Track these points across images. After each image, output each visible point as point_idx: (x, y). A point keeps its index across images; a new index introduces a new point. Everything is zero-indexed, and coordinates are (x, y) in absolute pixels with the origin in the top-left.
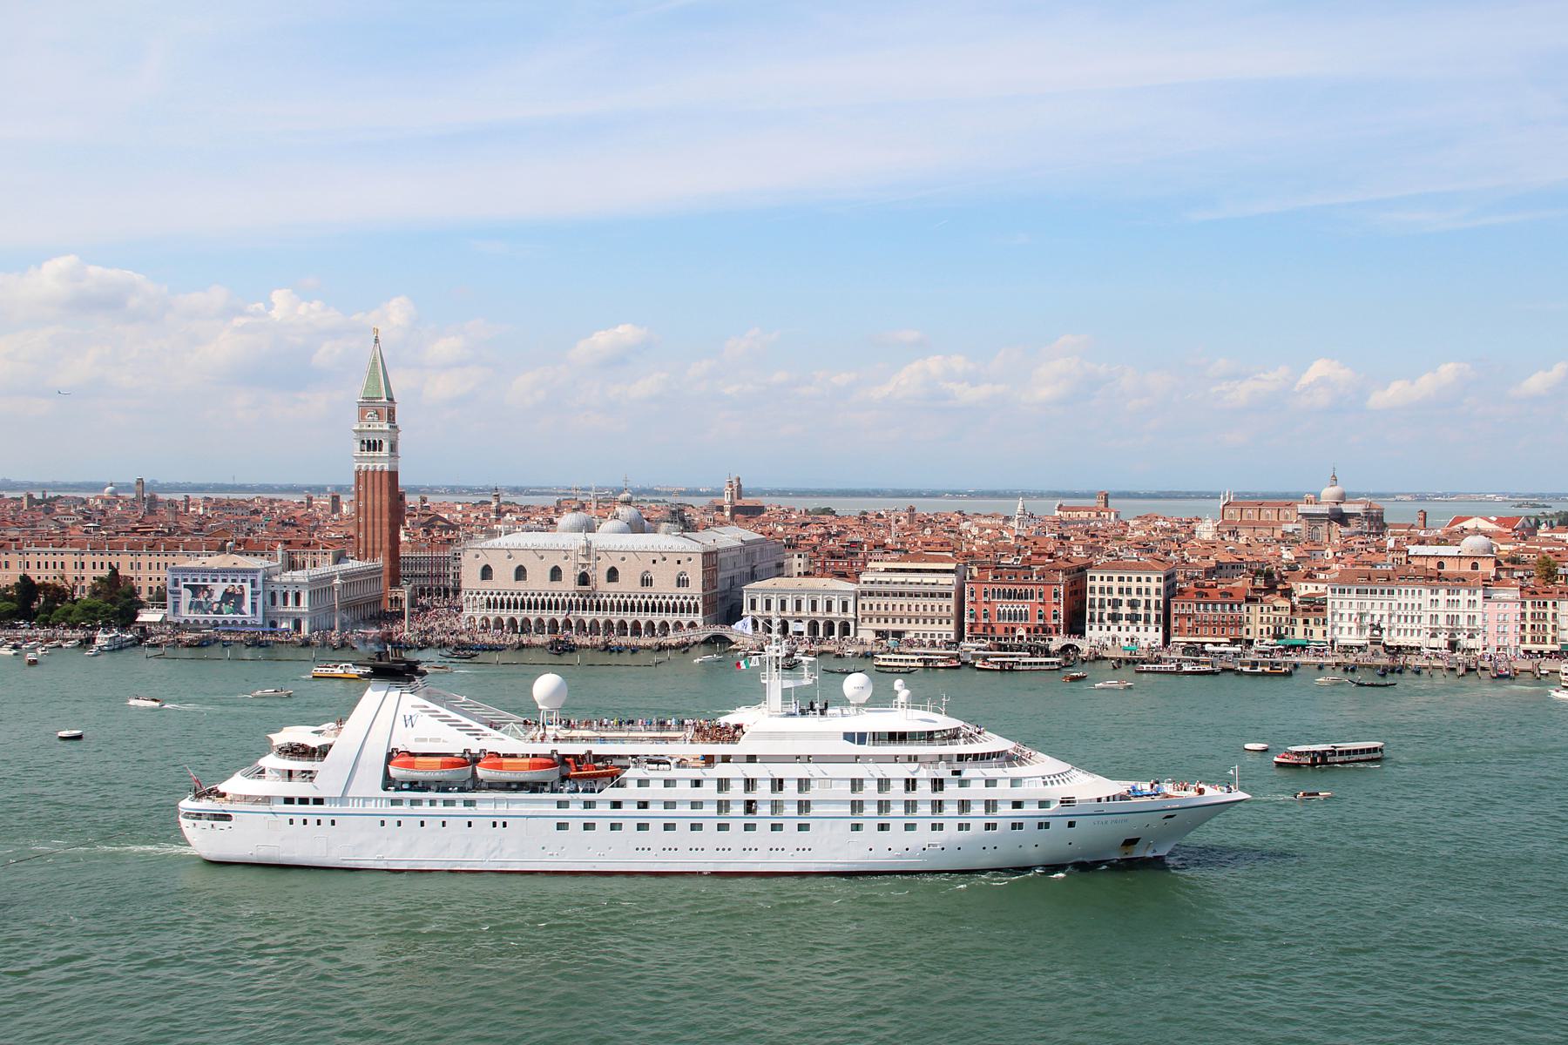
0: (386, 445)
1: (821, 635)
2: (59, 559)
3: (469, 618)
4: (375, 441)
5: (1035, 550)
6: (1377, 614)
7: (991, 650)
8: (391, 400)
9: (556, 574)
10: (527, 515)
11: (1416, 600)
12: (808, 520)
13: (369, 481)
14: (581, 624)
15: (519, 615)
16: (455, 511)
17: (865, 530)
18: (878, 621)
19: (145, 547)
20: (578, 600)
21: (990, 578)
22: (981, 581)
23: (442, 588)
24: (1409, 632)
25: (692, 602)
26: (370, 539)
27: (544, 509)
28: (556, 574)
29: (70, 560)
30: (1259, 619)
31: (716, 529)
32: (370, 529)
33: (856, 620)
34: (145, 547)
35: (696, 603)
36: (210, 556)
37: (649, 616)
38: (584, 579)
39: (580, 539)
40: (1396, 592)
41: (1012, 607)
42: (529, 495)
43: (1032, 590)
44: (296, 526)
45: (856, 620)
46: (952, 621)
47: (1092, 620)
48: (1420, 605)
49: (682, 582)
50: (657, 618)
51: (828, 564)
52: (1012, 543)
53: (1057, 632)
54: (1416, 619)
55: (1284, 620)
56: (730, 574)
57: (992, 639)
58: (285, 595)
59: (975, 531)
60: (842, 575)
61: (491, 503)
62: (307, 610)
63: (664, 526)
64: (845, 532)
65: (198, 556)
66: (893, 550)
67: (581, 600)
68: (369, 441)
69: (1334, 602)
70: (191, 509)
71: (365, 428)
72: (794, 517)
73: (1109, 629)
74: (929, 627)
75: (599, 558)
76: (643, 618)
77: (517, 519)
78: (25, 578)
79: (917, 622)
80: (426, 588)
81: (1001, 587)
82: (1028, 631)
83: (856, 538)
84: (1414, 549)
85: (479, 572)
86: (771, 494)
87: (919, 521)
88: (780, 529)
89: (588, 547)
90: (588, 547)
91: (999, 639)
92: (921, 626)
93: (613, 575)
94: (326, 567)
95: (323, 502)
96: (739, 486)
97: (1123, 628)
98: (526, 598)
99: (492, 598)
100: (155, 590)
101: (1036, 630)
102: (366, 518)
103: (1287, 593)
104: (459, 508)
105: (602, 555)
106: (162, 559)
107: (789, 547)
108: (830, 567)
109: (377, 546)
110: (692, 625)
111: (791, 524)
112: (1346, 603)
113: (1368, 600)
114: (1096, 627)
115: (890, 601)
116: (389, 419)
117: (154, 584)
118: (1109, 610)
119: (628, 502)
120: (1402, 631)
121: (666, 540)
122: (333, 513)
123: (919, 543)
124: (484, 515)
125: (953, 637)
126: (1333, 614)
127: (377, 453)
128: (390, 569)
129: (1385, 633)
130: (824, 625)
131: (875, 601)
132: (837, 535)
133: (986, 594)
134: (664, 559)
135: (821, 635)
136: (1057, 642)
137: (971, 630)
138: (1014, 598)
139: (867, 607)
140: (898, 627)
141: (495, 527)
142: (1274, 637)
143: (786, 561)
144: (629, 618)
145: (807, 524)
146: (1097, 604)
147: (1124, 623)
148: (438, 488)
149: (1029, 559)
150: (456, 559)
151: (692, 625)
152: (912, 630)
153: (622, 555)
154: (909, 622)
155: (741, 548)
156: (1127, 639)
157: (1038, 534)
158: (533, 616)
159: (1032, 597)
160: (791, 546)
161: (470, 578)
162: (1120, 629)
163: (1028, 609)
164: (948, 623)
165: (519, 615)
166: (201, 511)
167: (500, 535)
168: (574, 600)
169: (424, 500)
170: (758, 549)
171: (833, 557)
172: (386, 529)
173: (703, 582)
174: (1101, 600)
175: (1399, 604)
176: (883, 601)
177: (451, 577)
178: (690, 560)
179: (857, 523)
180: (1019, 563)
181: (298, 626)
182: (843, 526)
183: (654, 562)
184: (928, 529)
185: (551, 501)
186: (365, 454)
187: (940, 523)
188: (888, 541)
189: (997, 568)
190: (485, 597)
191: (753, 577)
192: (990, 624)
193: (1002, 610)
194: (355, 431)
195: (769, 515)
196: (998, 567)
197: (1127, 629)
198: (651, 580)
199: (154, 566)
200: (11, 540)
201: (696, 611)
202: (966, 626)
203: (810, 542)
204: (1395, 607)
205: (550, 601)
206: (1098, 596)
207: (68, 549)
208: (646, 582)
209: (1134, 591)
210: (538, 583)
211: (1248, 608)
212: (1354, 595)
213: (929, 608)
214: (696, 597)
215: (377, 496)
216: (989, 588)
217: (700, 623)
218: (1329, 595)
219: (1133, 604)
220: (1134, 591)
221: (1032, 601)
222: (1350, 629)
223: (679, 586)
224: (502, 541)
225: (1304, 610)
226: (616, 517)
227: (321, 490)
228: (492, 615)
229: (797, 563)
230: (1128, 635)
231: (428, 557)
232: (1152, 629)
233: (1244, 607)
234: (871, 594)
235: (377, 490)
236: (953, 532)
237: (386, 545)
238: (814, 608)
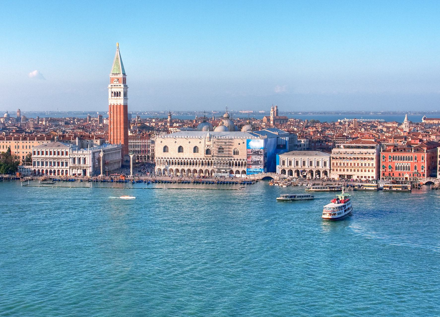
4: (117, 92)
8: (124, 74)
9: (196, 149)
13: (115, 109)
23: (146, 156)
26: (115, 135)
32: (115, 130)
38: (208, 152)
43: (412, 157)
52: (402, 135)
53: (424, 175)
58: (80, 159)
68: (115, 92)
80: (140, 156)
85: (163, 149)
92: (360, 174)
100: (25, 158)
102: (114, 125)
106: (28, 144)
109: (119, 138)
116: (123, 82)
117: (25, 155)
125: (375, 178)
132: (322, 132)
133: (390, 159)
137: (384, 174)
138: (404, 160)
140: (349, 173)
150: (152, 143)
159: (412, 160)
161: (159, 153)
163: (410, 165)
164: (372, 171)
167: (172, 133)
172: (122, 130)
177: (151, 151)
180: (405, 144)
181: (85, 172)
183: (239, 144)
186: (113, 98)
193: (397, 165)
198: (238, 152)
202: (381, 173)
210: (188, 154)
215: (118, 116)
221: (412, 161)
231: (140, 142)
235: (118, 113)
237: (122, 137)
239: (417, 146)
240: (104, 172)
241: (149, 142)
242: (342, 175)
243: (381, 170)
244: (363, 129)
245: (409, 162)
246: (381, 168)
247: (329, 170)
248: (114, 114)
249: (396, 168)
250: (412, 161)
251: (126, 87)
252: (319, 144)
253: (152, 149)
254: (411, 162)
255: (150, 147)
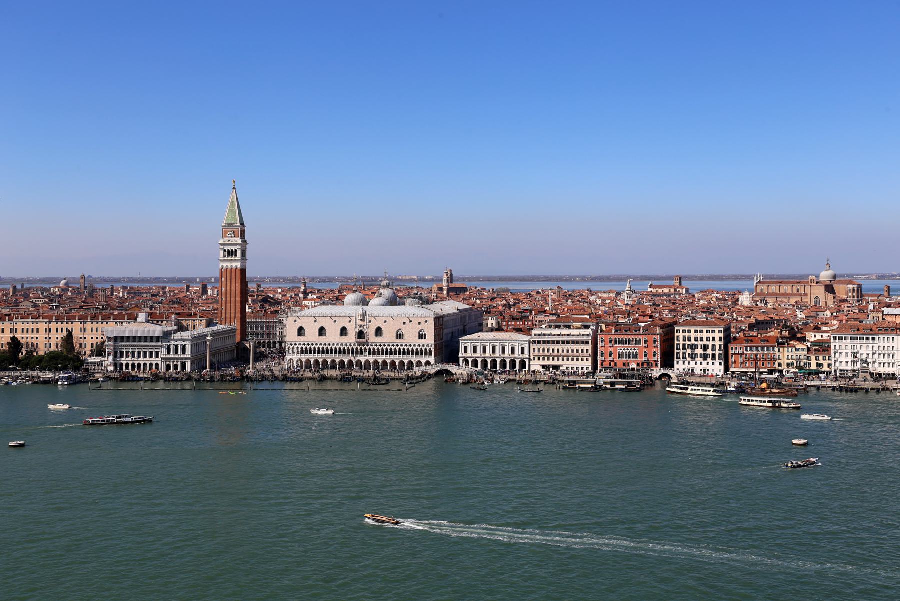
0: (239, 252)
1: (508, 368)
2: (35, 326)
3: (290, 360)
4: (232, 250)
5: (641, 313)
6: (865, 352)
7: (616, 378)
8: (242, 224)
9: (344, 331)
10: (322, 294)
11: (891, 344)
12: (495, 296)
13: (229, 275)
14: (359, 362)
15: (321, 358)
16: (277, 293)
17: (531, 301)
18: (544, 359)
19: (89, 318)
20: (357, 348)
21: (613, 331)
22: (609, 332)
23: (272, 341)
24: (887, 364)
25: (428, 348)
26: (228, 311)
27: (332, 291)
28: (344, 331)
29: (42, 326)
30: (786, 357)
31: (441, 302)
32: (228, 305)
33: (530, 359)
34: (89, 318)
35: (430, 349)
36: (130, 323)
37: (402, 357)
38: (361, 334)
39: (359, 309)
40: (877, 338)
41: (628, 349)
42: (322, 282)
43: (640, 339)
44: (181, 303)
45: (530, 359)
46: (590, 359)
47: (678, 358)
48: (893, 347)
49: (422, 336)
50: (406, 359)
51: (510, 323)
52: (624, 309)
53: (657, 365)
54: (891, 356)
55: (803, 357)
56: (450, 330)
57: (615, 370)
58: (177, 347)
59: (599, 301)
60: (519, 330)
61: (301, 288)
62: (190, 356)
63: (409, 301)
64: (519, 303)
65: (122, 323)
66: (551, 314)
67: (359, 347)
68: (229, 250)
69: (835, 344)
70: (115, 293)
71: (226, 242)
72: (486, 294)
73: (689, 363)
74: (575, 363)
75: (370, 321)
76: (397, 359)
77: (317, 298)
78: (14, 339)
79: (568, 359)
80: (262, 341)
81: (621, 337)
82: (638, 365)
83: (527, 307)
84: (886, 311)
86: (471, 279)
87: (564, 296)
88: (478, 301)
89: (364, 315)
90: (364, 315)
91: (620, 370)
92: (570, 362)
93: (379, 332)
94: (201, 328)
95: (195, 288)
96: (452, 275)
97: (699, 363)
98: (325, 347)
99: (304, 347)
101: (643, 364)
103: (803, 339)
104: (280, 290)
105: (373, 319)
107: (486, 313)
108: (512, 325)
109: (233, 315)
110: (428, 363)
111: (485, 298)
112: (844, 346)
113: (858, 344)
114: (681, 362)
115: (551, 346)
117: (95, 341)
118: (689, 351)
119: (387, 286)
120: (882, 364)
121: (410, 309)
122: (203, 295)
123: (566, 310)
124: (295, 295)
125: (590, 369)
126: (835, 353)
127: (234, 258)
128: (241, 329)
129: (871, 365)
130: (510, 362)
131: (541, 346)
132: (515, 304)
134: (411, 321)
135: (508, 368)
136: (657, 372)
137: (602, 364)
139: (537, 350)
140: (556, 363)
141: (304, 302)
142: (797, 367)
143: (484, 321)
144: (389, 359)
145: (494, 298)
146: (681, 347)
147: (699, 359)
148: (265, 278)
149: (637, 319)
150: (280, 323)
151: (428, 363)
152: (565, 364)
153: (384, 319)
154: (563, 359)
155: (457, 314)
156: (701, 370)
157: (639, 302)
158: (329, 358)
159: (640, 343)
160: (488, 311)
161: (291, 335)
162: (696, 363)
163: (638, 351)
165: (321, 358)
166: (121, 295)
168: (355, 347)
169: (259, 286)
170: (468, 315)
171: (513, 319)
172: (238, 305)
173: (435, 336)
174: (684, 345)
175: (879, 346)
176: (546, 347)
177: (278, 334)
178: (426, 321)
179: (525, 297)
180: (631, 321)
181: (184, 366)
182: (516, 299)
183: (405, 323)
184: (570, 301)
185: (336, 286)
186: (226, 258)
187: (577, 297)
188: (547, 308)
189: (618, 325)
190: (300, 347)
191: (465, 333)
192: (613, 361)
193: (621, 351)
194: (220, 244)
195: (470, 293)
196: (617, 324)
197: (701, 363)
198: (403, 335)
199: (95, 330)
200: (6, 315)
201: (431, 354)
202: (599, 362)
203: (497, 310)
204: (876, 348)
205: (311, 348)
206: (682, 342)
207: (41, 320)
208: (399, 336)
209: (705, 339)
210: (333, 337)
211: (779, 350)
212: (849, 341)
213: (575, 351)
214: (430, 345)
215: (233, 284)
216: (613, 337)
217: (433, 362)
218: (832, 339)
219: (705, 347)
220: (705, 339)
222: (847, 362)
223: (419, 338)
224: (311, 311)
225: (816, 350)
226: (380, 295)
227: (193, 280)
228: (304, 357)
229: (491, 322)
230: (702, 367)
232: (717, 363)
233: (776, 349)
234: (539, 342)
235: (233, 280)
236: (586, 302)
237: (239, 315)
238: (504, 352)
239: (647, 324)
240: (212, 366)
241: (276, 322)
242: (547, 366)
243: (598, 358)
244: (570, 301)
245: (637, 347)
246: (599, 355)
247: (528, 360)
248: (227, 281)
249: (619, 355)
250: (641, 345)
251: (244, 241)
252: (513, 323)
253: (280, 332)
254: (638, 347)
255: (278, 329)
